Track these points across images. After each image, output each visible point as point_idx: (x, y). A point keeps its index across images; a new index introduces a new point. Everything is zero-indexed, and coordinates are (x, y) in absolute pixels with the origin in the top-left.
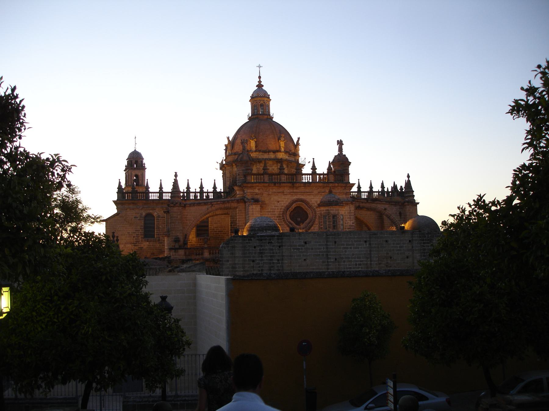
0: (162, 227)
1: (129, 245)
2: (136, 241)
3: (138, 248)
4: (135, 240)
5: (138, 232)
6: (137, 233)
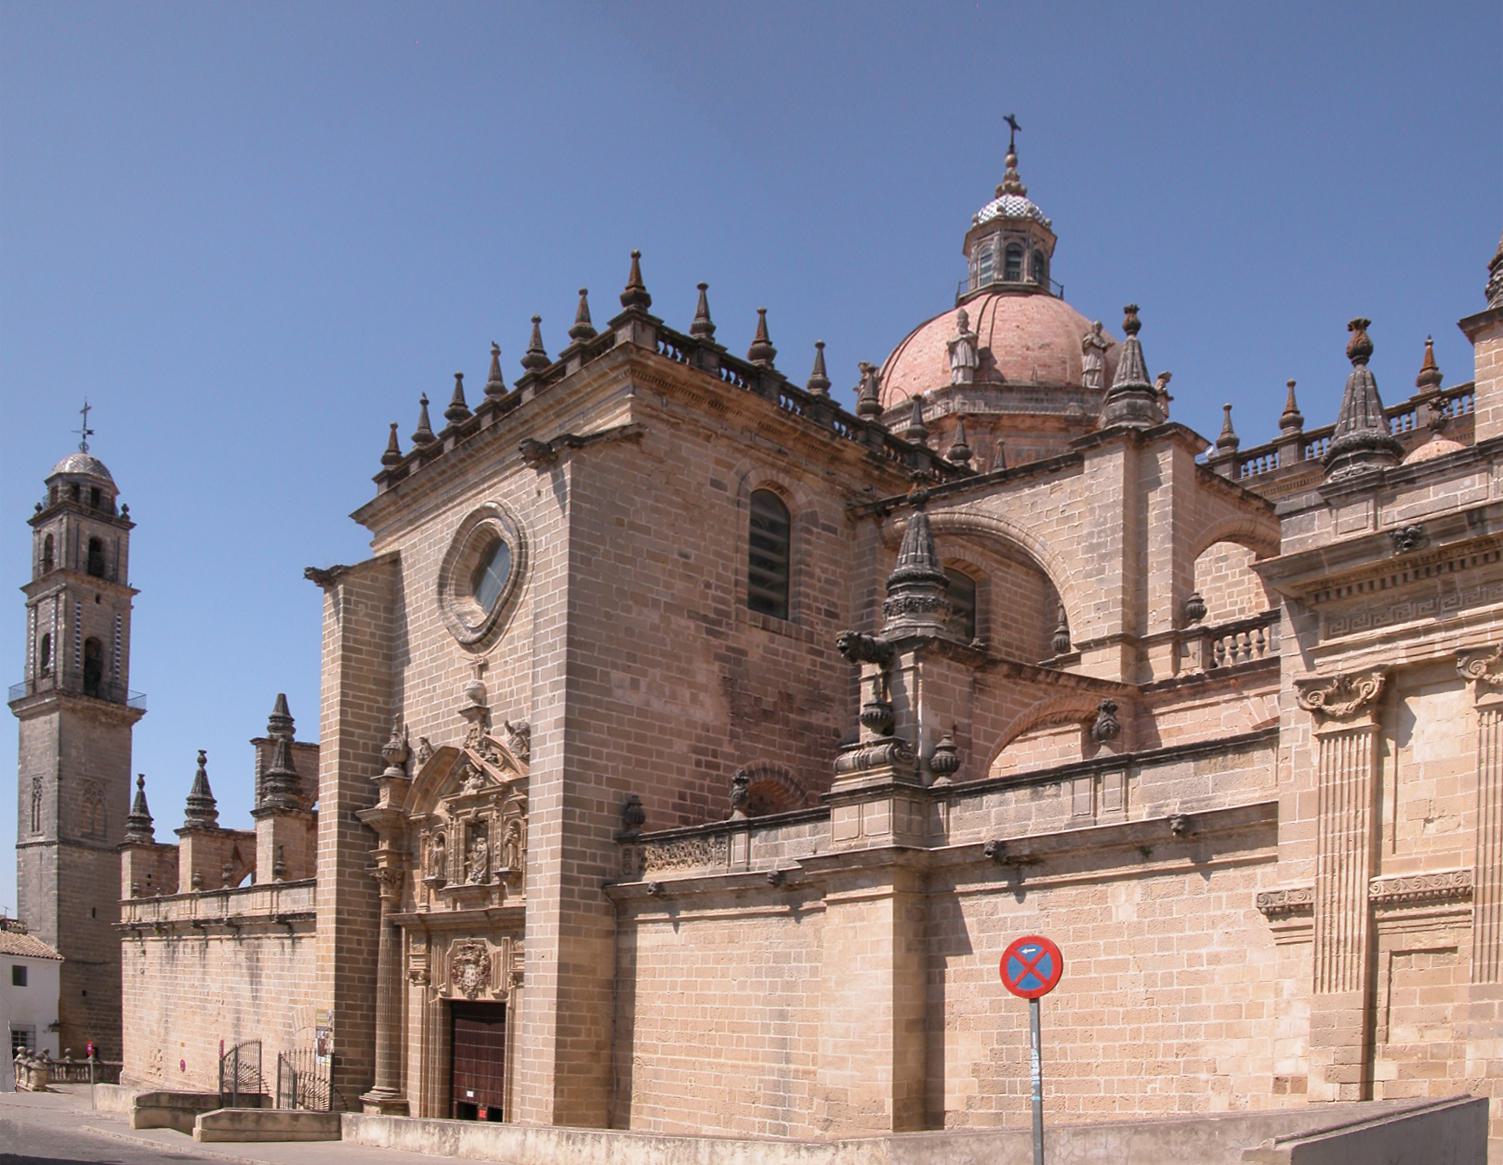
0: (823, 576)
1: (683, 622)
2: (717, 611)
3: (723, 651)
4: (709, 602)
5: (725, 568)
6: (720, 570)
